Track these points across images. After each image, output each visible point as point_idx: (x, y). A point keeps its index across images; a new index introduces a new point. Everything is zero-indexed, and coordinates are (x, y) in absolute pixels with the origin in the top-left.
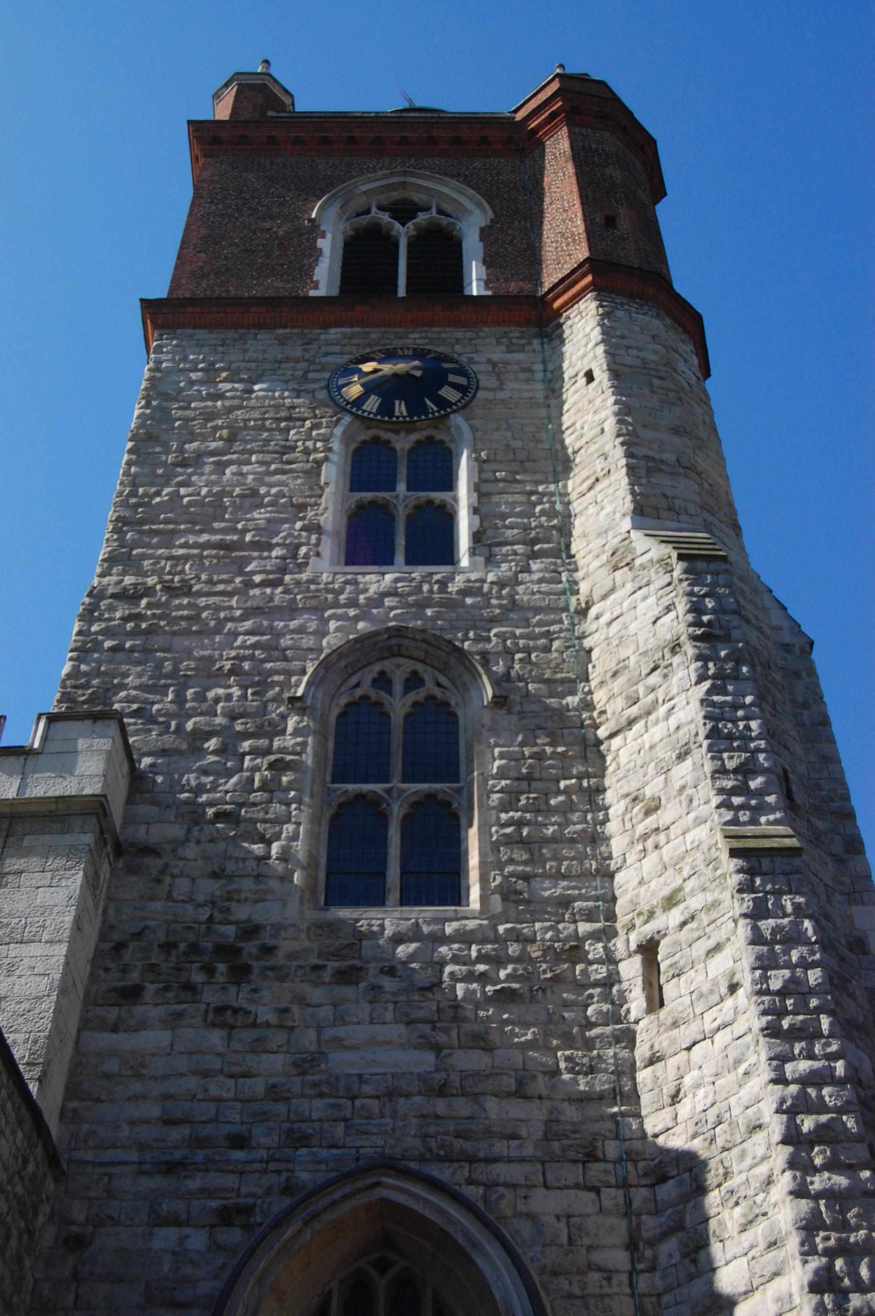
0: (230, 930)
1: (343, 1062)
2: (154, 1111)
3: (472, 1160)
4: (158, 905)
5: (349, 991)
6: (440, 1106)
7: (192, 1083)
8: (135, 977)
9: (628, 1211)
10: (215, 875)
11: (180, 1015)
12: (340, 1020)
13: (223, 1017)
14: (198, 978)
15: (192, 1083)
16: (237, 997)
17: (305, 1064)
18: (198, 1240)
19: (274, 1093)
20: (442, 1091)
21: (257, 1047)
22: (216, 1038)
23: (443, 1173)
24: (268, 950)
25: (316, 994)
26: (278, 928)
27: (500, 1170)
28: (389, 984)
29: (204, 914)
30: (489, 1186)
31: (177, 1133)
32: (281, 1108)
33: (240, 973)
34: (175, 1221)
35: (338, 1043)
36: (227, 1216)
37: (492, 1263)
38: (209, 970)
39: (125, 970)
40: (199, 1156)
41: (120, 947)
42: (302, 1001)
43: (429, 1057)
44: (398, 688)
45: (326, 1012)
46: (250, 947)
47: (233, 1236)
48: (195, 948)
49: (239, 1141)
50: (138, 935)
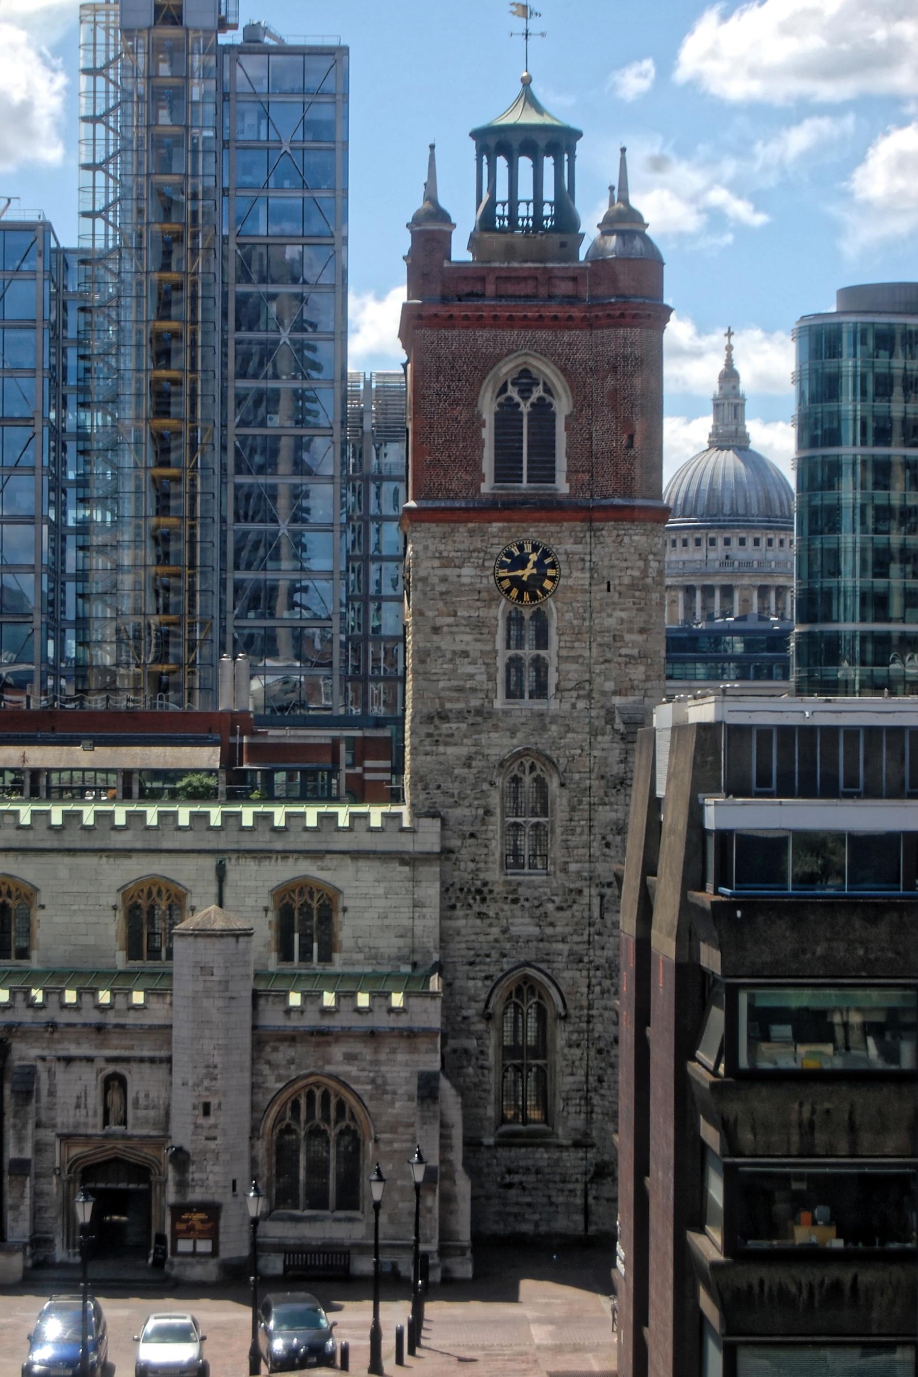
0: (479, 883)
1: (514, 930)
2: (463, 946)
3: (549, 961)
4: (456, 873)
5: (514, 906)
6: (541, 945)
7: (473, 937)
8: (453, 901)
9: (589, 977)
10: (473, 861)
11: (468, 915)
12: (513, 916)
13: (481, 915)
14: (471, 901)
15: (473, 937)
16: (484, 909)
17: (505, 931)
18: (480, 984)
19: (496, 941)
20: (542, 940)
21: (491, 925)
22: (478, 922)
23: (543, 966)
24: (491, 892)
25: (506, 907)
26: (494, 883)
27: (555, 965)
28: (527, 904)
29: (470, 877)
30: (553, 969)
31: (472, 952)
32: (497, 945)
33: (484, 900)
34: (474, 979)
35: (512, 924)
36: (487, 978)
37: (553, 991)
38: (474, 899)
39: (450, 898)
40: (478, 960)
41: (447, 890)
42: (502, 910)
43: (538, 929)
44: (527, 772)
45: (509, 913)
46: (486, 890)
47: (488, 983)
48: (469, 891)
49: (488, 956)
50: (452, 885)
